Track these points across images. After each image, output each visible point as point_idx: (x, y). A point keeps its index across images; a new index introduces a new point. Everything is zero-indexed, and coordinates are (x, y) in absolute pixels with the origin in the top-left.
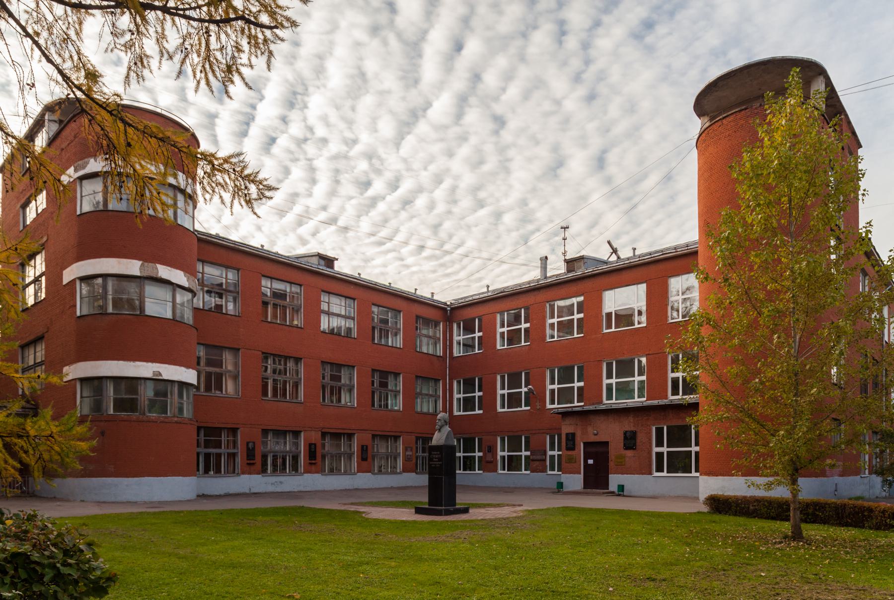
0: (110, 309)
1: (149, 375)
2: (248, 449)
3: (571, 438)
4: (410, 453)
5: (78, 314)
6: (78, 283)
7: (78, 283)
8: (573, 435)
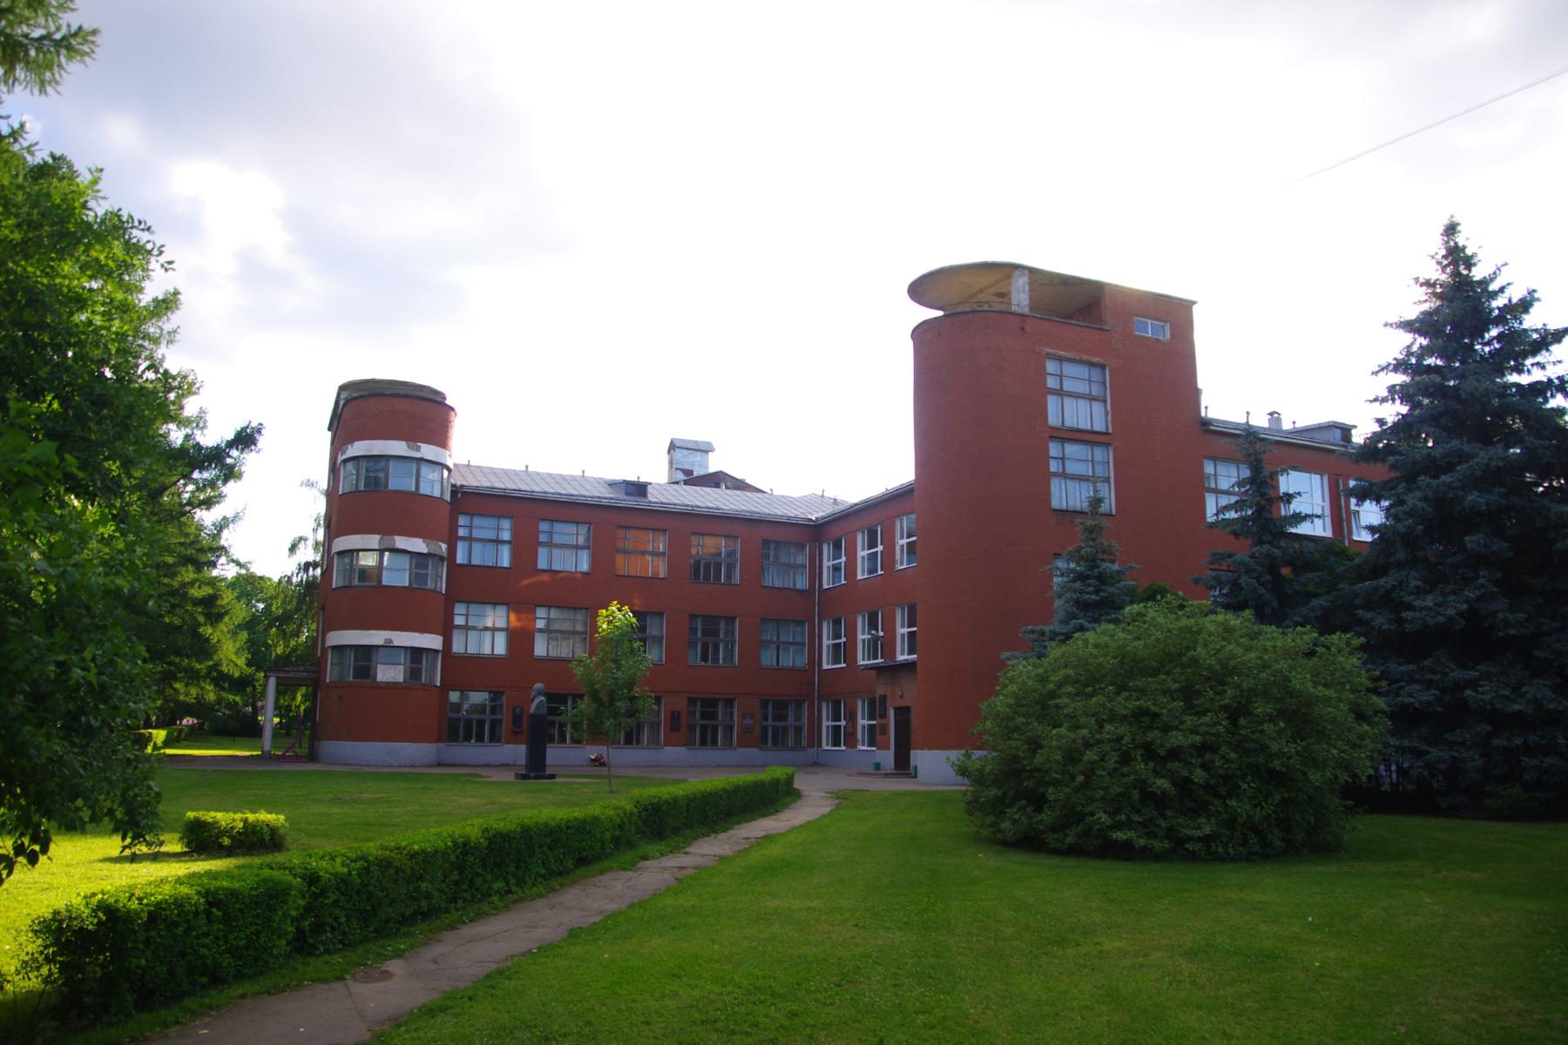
0: (356, 582)
1: (380, 642)
2: (514, 715)
3: (883, 698)
4: (751, 722)
5: (334, 586)
6: (336, 557)
7: (336, 557)
8: (885, 696)
